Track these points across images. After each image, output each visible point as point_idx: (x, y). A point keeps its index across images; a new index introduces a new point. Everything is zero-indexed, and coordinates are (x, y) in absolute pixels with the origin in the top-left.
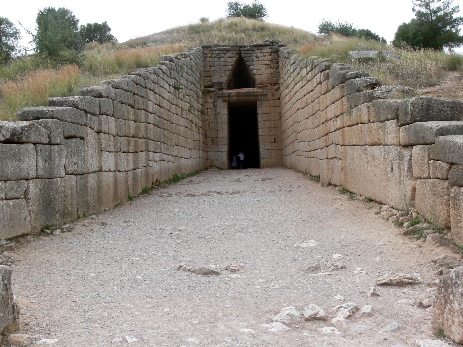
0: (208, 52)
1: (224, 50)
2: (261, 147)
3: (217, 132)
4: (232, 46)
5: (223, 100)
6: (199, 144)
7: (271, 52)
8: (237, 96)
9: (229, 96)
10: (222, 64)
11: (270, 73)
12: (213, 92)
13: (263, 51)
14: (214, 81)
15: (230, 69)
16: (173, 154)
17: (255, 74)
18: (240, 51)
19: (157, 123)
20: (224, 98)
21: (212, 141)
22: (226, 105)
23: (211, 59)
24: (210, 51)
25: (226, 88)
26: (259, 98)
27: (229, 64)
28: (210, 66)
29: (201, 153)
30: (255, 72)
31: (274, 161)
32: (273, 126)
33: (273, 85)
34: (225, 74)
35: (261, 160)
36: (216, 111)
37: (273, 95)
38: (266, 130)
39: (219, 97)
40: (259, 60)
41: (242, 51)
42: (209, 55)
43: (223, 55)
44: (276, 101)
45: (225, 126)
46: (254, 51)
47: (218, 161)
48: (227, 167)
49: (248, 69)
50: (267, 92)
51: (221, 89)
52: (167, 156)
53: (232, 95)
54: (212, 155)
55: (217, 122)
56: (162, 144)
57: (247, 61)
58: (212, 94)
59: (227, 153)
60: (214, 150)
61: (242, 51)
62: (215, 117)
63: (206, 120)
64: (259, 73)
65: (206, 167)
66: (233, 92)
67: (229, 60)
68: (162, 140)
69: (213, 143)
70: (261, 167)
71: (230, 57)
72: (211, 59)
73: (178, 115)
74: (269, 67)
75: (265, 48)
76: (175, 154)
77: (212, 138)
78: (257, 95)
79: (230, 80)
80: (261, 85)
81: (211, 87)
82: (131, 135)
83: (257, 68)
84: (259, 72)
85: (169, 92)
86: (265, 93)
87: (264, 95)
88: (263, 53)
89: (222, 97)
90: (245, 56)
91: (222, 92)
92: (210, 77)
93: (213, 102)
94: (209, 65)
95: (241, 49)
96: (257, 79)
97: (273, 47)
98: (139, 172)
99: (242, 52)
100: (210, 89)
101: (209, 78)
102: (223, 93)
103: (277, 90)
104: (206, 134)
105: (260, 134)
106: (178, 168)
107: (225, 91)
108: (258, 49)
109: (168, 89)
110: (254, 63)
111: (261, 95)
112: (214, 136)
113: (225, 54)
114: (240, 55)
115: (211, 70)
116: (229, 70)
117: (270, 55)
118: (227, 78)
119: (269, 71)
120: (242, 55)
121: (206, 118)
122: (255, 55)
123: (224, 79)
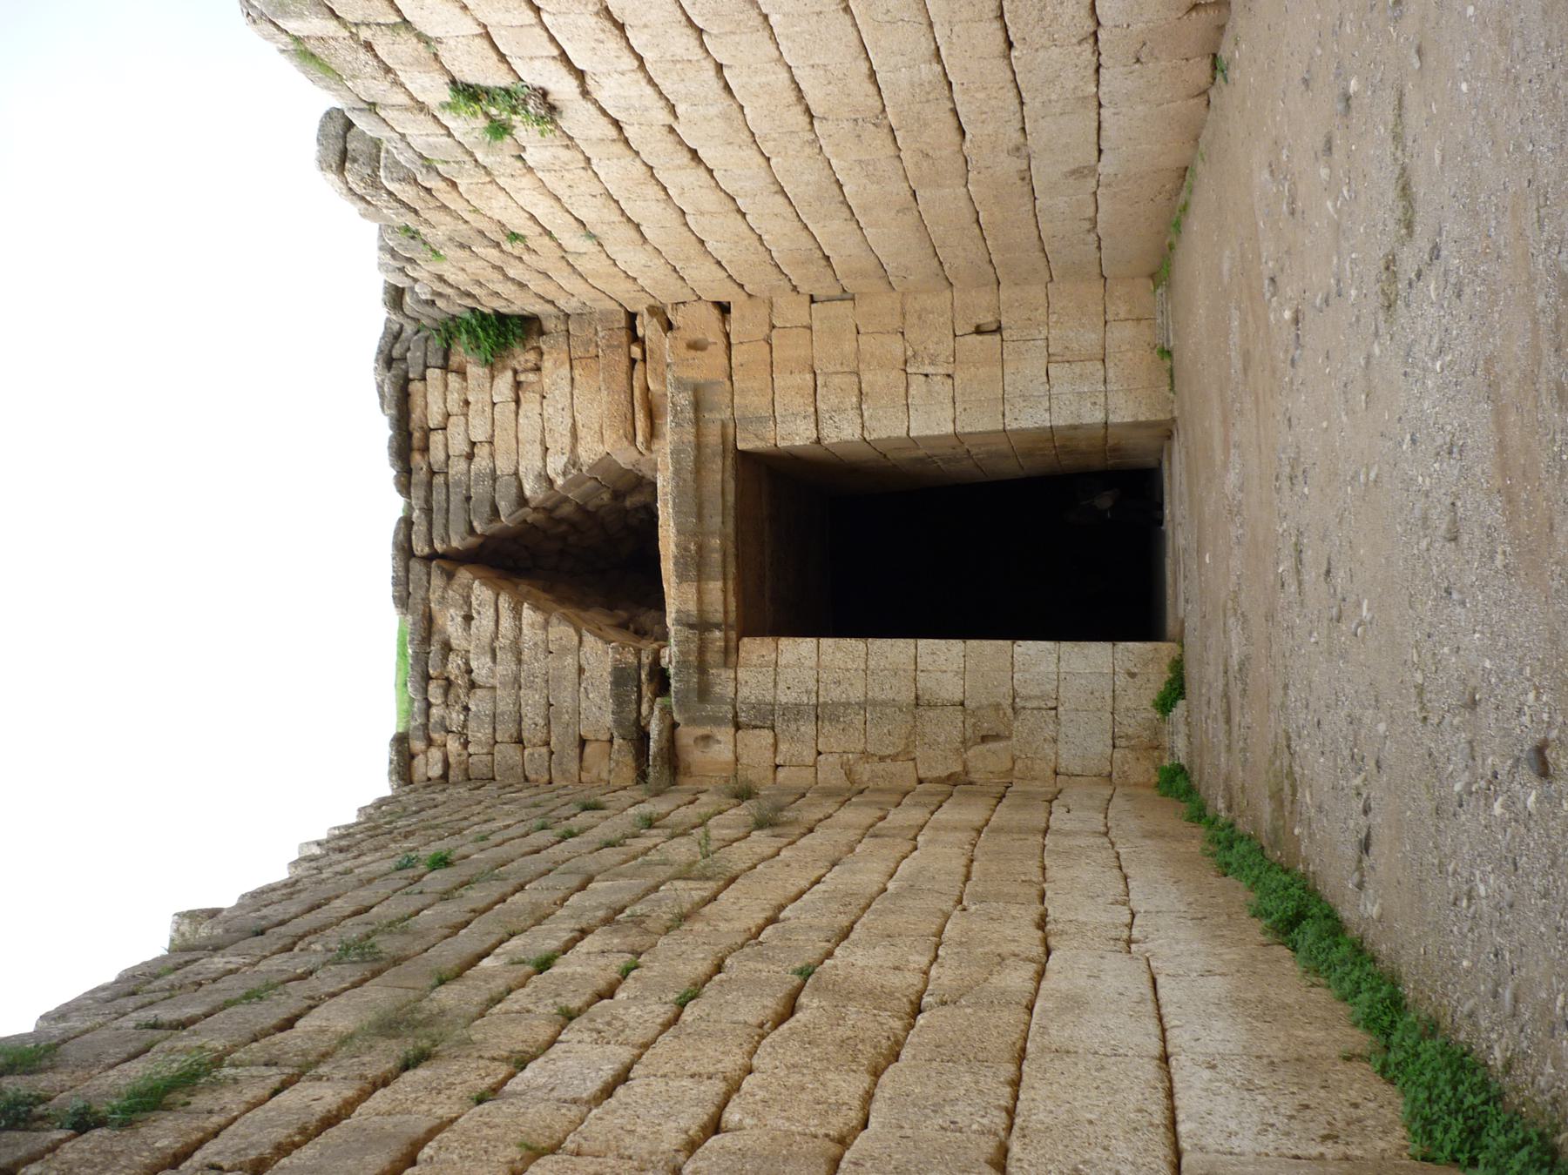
0: (435, 754)
1: (421, 659)
2: (1030, 418)
3: (931, 706)
4: (403, 600)
5: (726, 665)
6: (999, 830)
7: (445, 368)
8: (701, 578)
9: (700, 626)
10: (506, 666)
11: (565, 371)
12: (674, 725)
13: (434, 420)
14: (608, 719)
15: (539, 618)
17: (574, 462)
20: (713, 656)
21: (984, 739)
22: (755, 649)
23: (479, 734)
24: (430, 742)
25: (655, 646)
26: (713, 437)
27: (506, 622)
28: (519, 741)
30: (556, 464)
31: (1122, 334)
32: (896, 346)
33: (636, 351)
34: (564, 650)
35: (1113, 419)
36: (796, 711)
37: (695, 346)
38: (917, 384)
39: (704, 692)
40: (491, 443)
41: (431, 543)
42: (453, 745)
43: (454, 663)
44: (734, 326)
45: (893, 651)
46: (432, 473)
47: (1123, 704)
48: (1164, 647)
49: (548, 510)
50: (680, 384)
51: (661, 680)
53: (692, 607)
54: (1083, 742)
55: (863, 706)
57: (495, 511)
58: (687, 735)
59: (1066, 646)
60: (1049, 731)
61: (431, 543)
62: (834, 719)
63: (849, 774)
64: (567, 440)
66: (677, 596)
67: (483, 622)
69: (997, 737)
70: (1161, 416)
71: (468, 618)
72: (479, 734)
74: (532, 377)
75: (417, 401)
78: (699, 447)
79: (623, 626)
81: (643, 737)
83: (538, 449)
86: (684, 399)
87: (697, 406)
88: (448, 415)
89: (702, 669)
90: (463, 528)
91: (672, 671)
93: (738, 727)
95: (420, 548)
96: (601, 450)
97: (414, 356)
101: (588, 750)
102: (683, 664)
103: (669, 326)
104: (939, 780)
105: (948, 429)
107: (670, 655)
108: (425, 449)
110: (504, 466)
111: (697, 422)
112: (948, 729)
113: (447, 648)
114: (452, 561)
115: (541, 735)
116: (546, 625)
117: (462, 373)
118: (589, 639)
119: (555, 373)
122: (458, 467)
123: (600, 655)
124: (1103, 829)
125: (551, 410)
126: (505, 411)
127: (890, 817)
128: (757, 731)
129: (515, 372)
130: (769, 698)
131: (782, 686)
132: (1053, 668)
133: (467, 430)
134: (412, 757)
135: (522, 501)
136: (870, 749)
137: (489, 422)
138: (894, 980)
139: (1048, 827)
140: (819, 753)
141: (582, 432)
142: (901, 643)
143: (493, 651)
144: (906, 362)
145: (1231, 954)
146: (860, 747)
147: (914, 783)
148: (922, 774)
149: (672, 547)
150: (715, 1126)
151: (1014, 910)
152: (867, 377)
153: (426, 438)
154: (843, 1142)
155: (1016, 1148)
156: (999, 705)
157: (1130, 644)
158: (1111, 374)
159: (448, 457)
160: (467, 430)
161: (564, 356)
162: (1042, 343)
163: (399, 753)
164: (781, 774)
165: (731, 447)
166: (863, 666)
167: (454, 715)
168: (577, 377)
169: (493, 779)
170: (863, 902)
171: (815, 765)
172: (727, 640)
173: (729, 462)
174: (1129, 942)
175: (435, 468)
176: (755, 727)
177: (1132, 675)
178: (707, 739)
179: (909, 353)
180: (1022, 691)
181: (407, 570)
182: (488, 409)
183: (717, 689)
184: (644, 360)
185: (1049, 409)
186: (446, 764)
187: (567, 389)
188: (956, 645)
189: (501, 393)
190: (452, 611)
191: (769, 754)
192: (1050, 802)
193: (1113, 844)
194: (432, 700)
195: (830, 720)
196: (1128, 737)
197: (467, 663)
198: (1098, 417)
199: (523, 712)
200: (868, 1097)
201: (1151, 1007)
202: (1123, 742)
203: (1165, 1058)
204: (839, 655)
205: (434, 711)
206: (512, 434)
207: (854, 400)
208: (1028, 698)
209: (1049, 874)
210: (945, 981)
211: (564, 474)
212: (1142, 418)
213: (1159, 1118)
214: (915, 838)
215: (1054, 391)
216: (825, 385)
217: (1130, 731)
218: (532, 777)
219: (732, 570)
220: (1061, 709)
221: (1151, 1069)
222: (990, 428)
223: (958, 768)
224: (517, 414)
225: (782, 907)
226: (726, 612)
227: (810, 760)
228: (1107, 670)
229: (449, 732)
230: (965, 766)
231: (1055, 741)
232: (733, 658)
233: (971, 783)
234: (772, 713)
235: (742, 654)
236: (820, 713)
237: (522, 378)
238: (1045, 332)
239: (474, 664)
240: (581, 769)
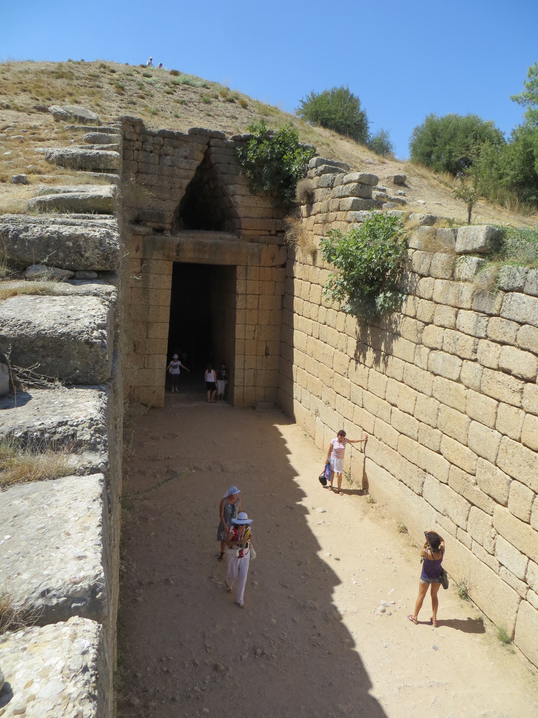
0: (135, 137)
22: (168, 267)
27: (182, 172)
33: (273, 232)
35: (235, 388)
36: (146, 280)
42: (138, 144)
45: (165, 315)
51: (160, 231)
67: (183, 164)
71: (186, 158)
72: (141, 156)
99: (213, 149)
105: (237, 336)
113: (175, 147)
131: (156, 276)
142: (168, 317)
158: (248, 388)
162: (261, 368)
166: (161, 304)
177: (154, 392)
181: (206, 136)
186: (130, 140)
188: (166, 336)
194: (155, 138)
198: (236, 383)
199: (149, 175)
205: (151, 138)
211: (235, 202)
212: (235, 396)
217: (136, 392)
220: (144, 370)
222: (236, 350)
229: (142, 143)
234: (147, 272)
235: (167, 262)
236: (145, 290)
238: (264, 369)
239: (168, 158)
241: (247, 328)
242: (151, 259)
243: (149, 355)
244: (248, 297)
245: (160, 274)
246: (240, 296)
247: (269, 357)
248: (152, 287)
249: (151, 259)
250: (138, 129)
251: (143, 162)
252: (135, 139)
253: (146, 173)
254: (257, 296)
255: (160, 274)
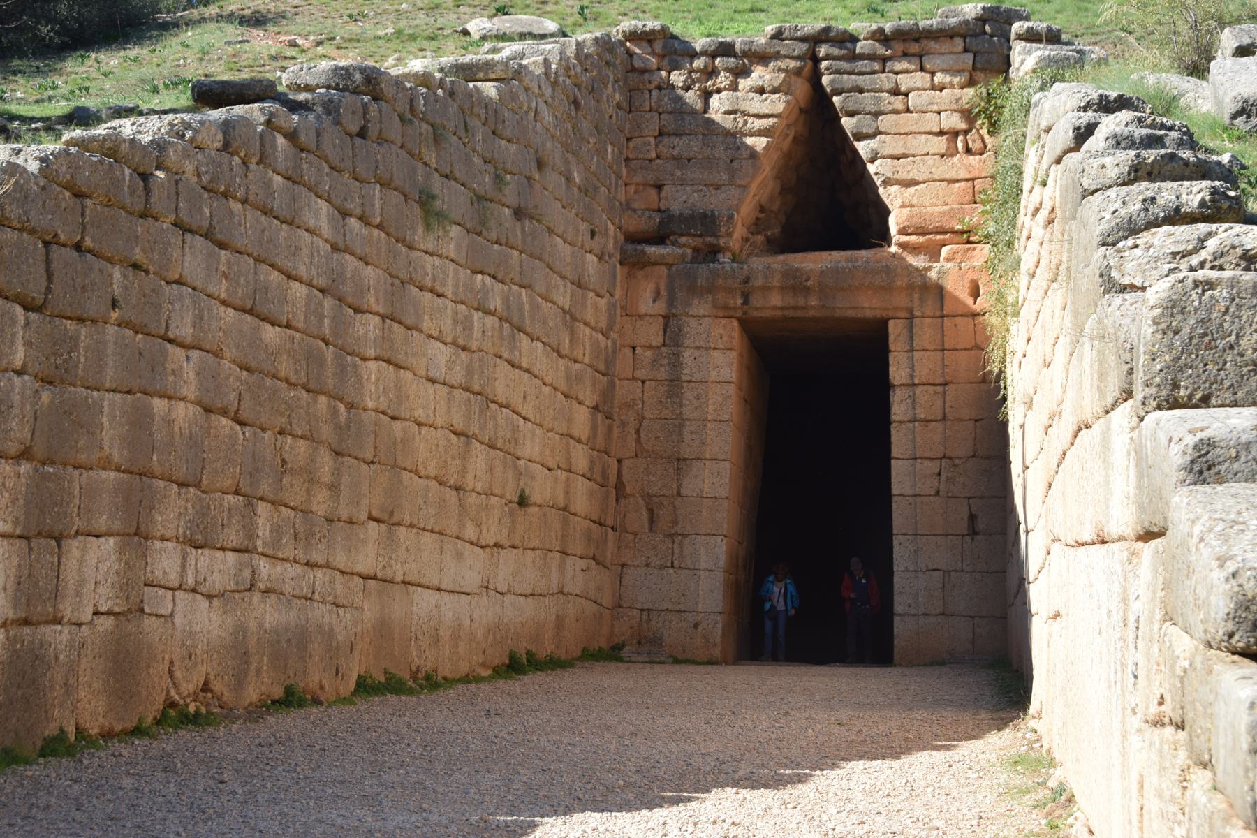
4: (778, 35)
16: (340, 560)
18: (816, 60)
19: (233, 396)
21: (651, 511)
29: (576, 574)
35: (897, 620)
36: (676, 364)
38: (933, 467)
40: (908, 110)
46: (885, 60)
48: (717, 653)
52: (293, 571)
56: (262, 508)
59: (721, 576)
60: (655, 561)
61: (824, 59)
63: (628, 406)
64: (903, 176)
65: (623, 643)
67: (758, 105)
68: (265, 488)
70: (896, 657)
71: (761, 91)
73: (398, 366)
74: (960, 145)
75: (945, 46)
76: (366, 560)
77: (648, 497)
80: (913, 238)
81: (660, 240)
82: (13, 448)
84: (906, 170)
85: (335, 248)
92: (659, 187)
94: (652, 127)
98: (65, 637)
99: (824, 64)
100: (651, 250)
101: (653, 192)
105: (896, 490)
106: (383, 630)
109: (326, 231)
117: (971, 83)
120: (825, 80)
121: (626, 390)
124: (566, 591)
125: (931, 162)
126: (932, 122)
127: (579, 446)
128: (661, 332)
129: (966, 132)
130: (687, 342)
131: (697, 353)
132: (703, 565)
133: (918, 89)
134: (650, 42)
135: (860, 137)
136: (645, 423)
137: (924, 109)
138: (470, 477)
139: (567, 554)
140: (643, 382)
141: (912, 190)
143: (735, 112)
144: (950, 458)
145: (480, 634)
146: (647, 415)
147: (618, 456)
148: (626, 463)
149: (811, 266)
150: (420, 424)
151: (506, 531)
152: (939, 427)
153: (913, 55)
154: (416, 472)
155: (414, 531)
156: (677, 523)
157: (720, 626)
158: (931, 620)
159: (897, 73)
160: (918, 89)
161: (975, 174)
163: (653, 31)
164: (628, 351)
165: (891, 314)
167: (682, 78)
168: (957, 185)
169: (630, 112)
170: (511, 450)
171: (634, 378)
172: (734, 309)
173: (878, 314)
174: (487, 587)
175: (888, 64)
176: (665, 331)
177: (696, 626)
178: (657, 296)
179: (957, 461)
180: (686, 541)
182: (935, 108)
183: (696, 301)
184: (969, 242)
185: (907, 570)
186: (644, 71)
187: (948, 176)
188: (723, 492)
189: (947, 118)
190: (768, 77)
191: (643, 342)
192: (594, 558)
193: (553, 594)
195: (668, 391)
196: (649, 620)
197: (725, 89)
199: (684, 138)
200: (428, 477)
201: (458, 589)
202: (645, 617)
203: (439, 589)
204: (720, 399)
206: (914, 128)
207: (922, 416)
208: (681, 545)
209: (529, 552)
210: (469, 500)
212: (896, 642)
213: (423, 581)
214: (559, 468)
215: (920, 574)
216: (936, 393)
217: (653, 623)
218: (631, 145)
219: (791, 313)
220: (671, 571)
221: (435, 582)
223: (628, 490)
224: (930, 133)
225: (507, 407)
226: (757, 309)
227: (638, 374)
228: (700, 607)
230: (633, 495)
231: (647, 565)
232: (720, 314)
233: (617, 500)
234: (677, 345)
235: (724, 321)
236: (674, 385)
237: (960, 138)
240: (637, 184)
241: (918, 466)
242: (687, 315)
243: (684, 536)
244: (918, 390)
245: (707, 349)
246: (898, 391)
247: (978, 538)
248: (688, 378)
249: (687, 315)
250: (658, 46)
251: (671, 113)
252: (655, 67)
253: (676, 135)
254: (939, 389)
255: (707, 349)
